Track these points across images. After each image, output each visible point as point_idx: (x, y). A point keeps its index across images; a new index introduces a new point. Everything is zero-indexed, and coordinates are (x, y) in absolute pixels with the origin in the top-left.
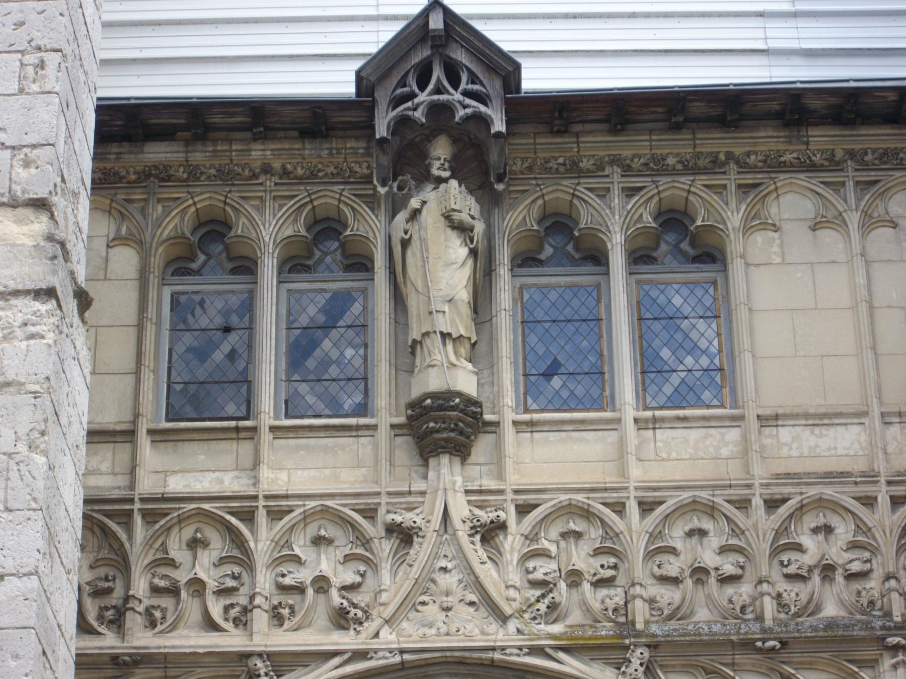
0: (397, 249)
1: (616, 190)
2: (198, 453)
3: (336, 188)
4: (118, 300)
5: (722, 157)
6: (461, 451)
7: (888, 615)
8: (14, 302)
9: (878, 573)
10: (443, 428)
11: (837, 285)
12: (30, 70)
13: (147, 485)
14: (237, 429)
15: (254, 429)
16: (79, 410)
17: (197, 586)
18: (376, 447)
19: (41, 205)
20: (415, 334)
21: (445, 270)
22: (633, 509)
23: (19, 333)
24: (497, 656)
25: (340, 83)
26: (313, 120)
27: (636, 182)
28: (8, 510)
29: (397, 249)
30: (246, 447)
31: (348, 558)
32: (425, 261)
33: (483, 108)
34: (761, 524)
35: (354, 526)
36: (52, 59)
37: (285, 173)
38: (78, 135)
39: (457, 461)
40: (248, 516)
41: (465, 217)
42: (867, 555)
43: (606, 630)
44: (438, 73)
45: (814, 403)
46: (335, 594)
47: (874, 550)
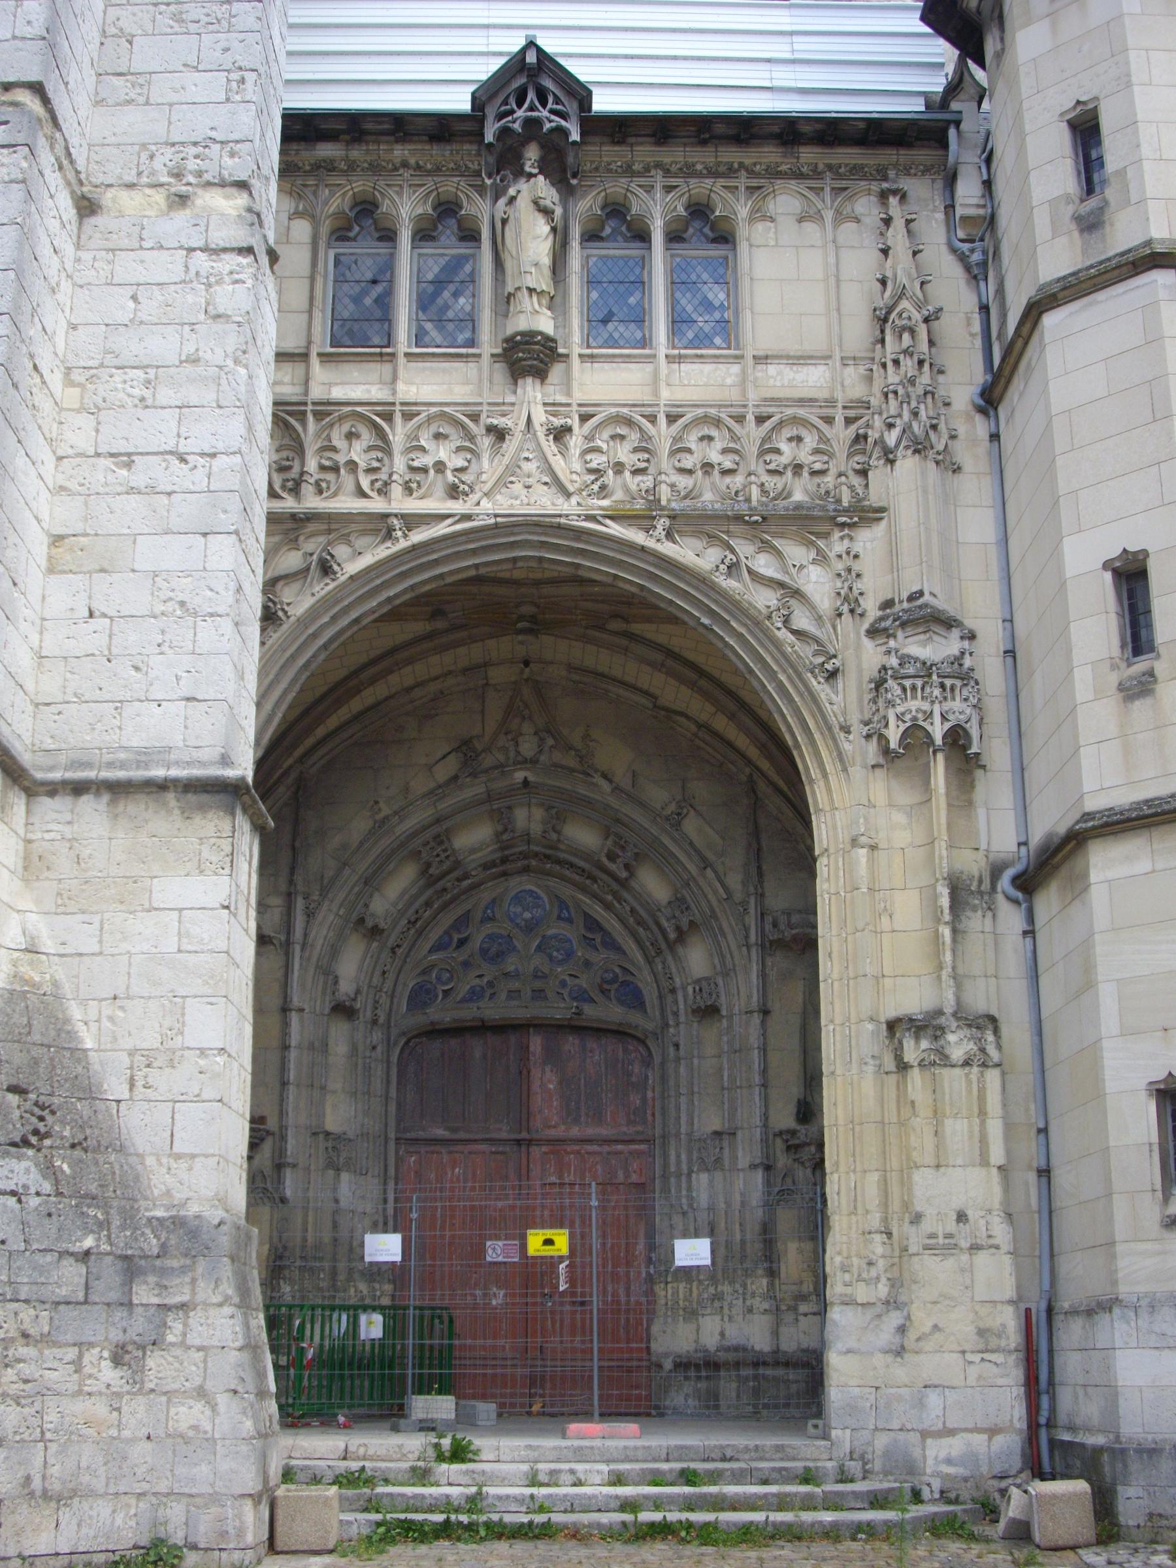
0: (499, 225)
1: (658, 187)
2: (353, 371)
3: (456, 179)
4: (297, 258)
5: (736, 166)
6: (541, 374)
7: (839, 501)
8: (223, 256)
9: (833, 471)
10: (529, 357)
11: (814, 263)
12: (234, 84)
13: (317, 392)
14: (381, 354)
15: (393, 355)
16: (269, 338)
17: (352, 465)
18: (480, 370)
19: (243, 185)
20: (510, 289)
21: (533, 242)
22: (662, 420)
23: (227, 279)
24: (563, 520)
25: (459, 102)
26: (439, 128)
27: (673, 182)
28: (220, 407)
29: (499, 225)
30: (387, 368)
31: (459, 449)
32: (518, 235)
33: (563, 123)
34: (752, 433)
35: (463, 427)
36: (250, 77)
37: (418, 167)
38: (269, 135)
39: (538, 382)
40: (388, 417)
41: (548, 203)
42: (826, 458)
43: (640, 505)
44: (531, 96)
45: (794, 348)
46: (449, 473)
47: (831, 455)
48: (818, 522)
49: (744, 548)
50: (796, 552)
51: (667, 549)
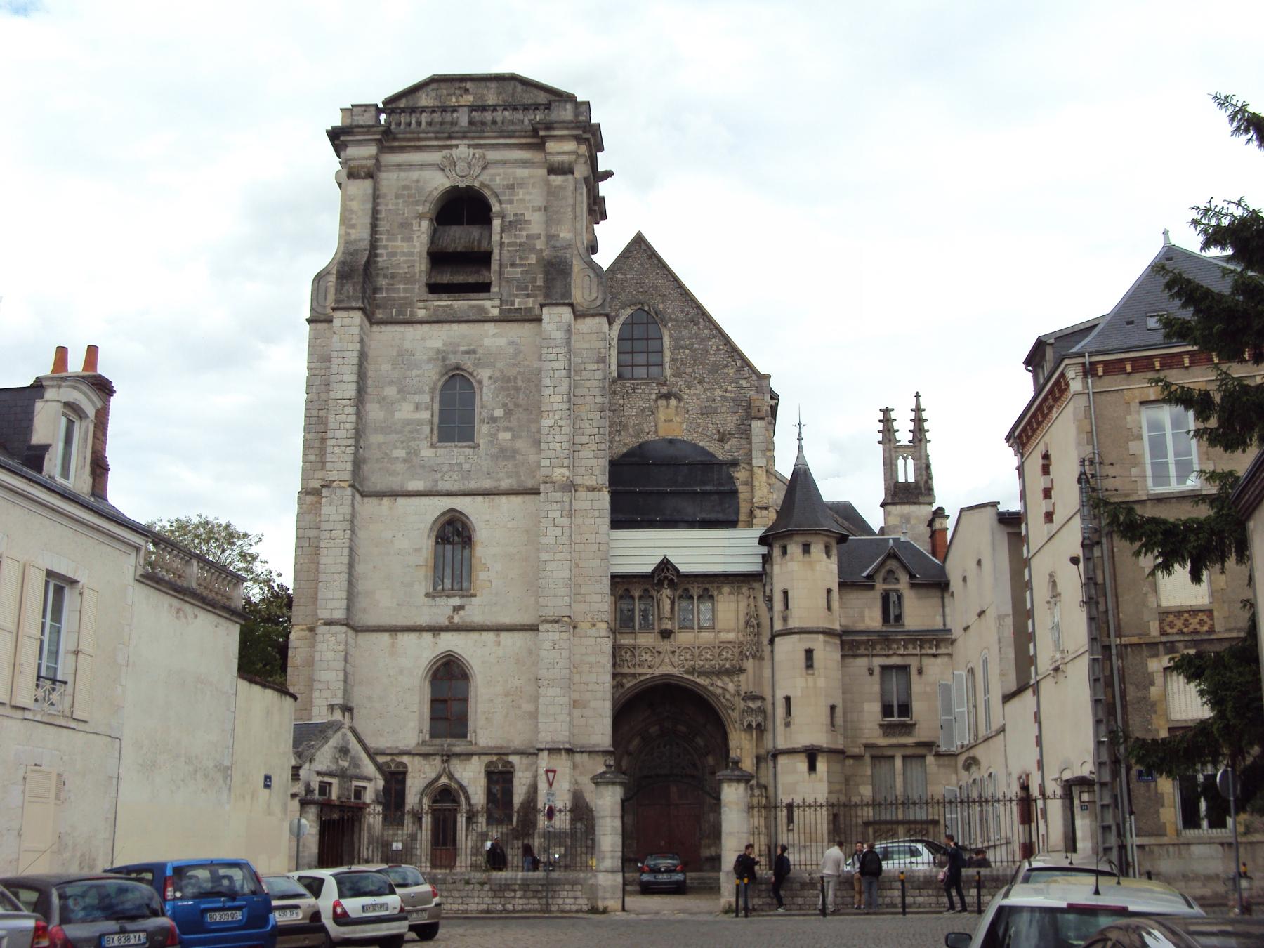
10: (666, 634)
11: (733, 605)
48: (730, 673)
49: (715, 678)
50: (726, 679)
51: (698, 680)
